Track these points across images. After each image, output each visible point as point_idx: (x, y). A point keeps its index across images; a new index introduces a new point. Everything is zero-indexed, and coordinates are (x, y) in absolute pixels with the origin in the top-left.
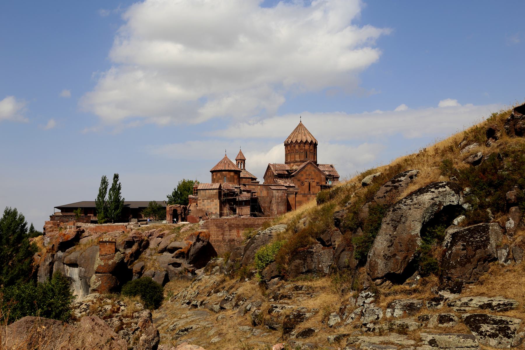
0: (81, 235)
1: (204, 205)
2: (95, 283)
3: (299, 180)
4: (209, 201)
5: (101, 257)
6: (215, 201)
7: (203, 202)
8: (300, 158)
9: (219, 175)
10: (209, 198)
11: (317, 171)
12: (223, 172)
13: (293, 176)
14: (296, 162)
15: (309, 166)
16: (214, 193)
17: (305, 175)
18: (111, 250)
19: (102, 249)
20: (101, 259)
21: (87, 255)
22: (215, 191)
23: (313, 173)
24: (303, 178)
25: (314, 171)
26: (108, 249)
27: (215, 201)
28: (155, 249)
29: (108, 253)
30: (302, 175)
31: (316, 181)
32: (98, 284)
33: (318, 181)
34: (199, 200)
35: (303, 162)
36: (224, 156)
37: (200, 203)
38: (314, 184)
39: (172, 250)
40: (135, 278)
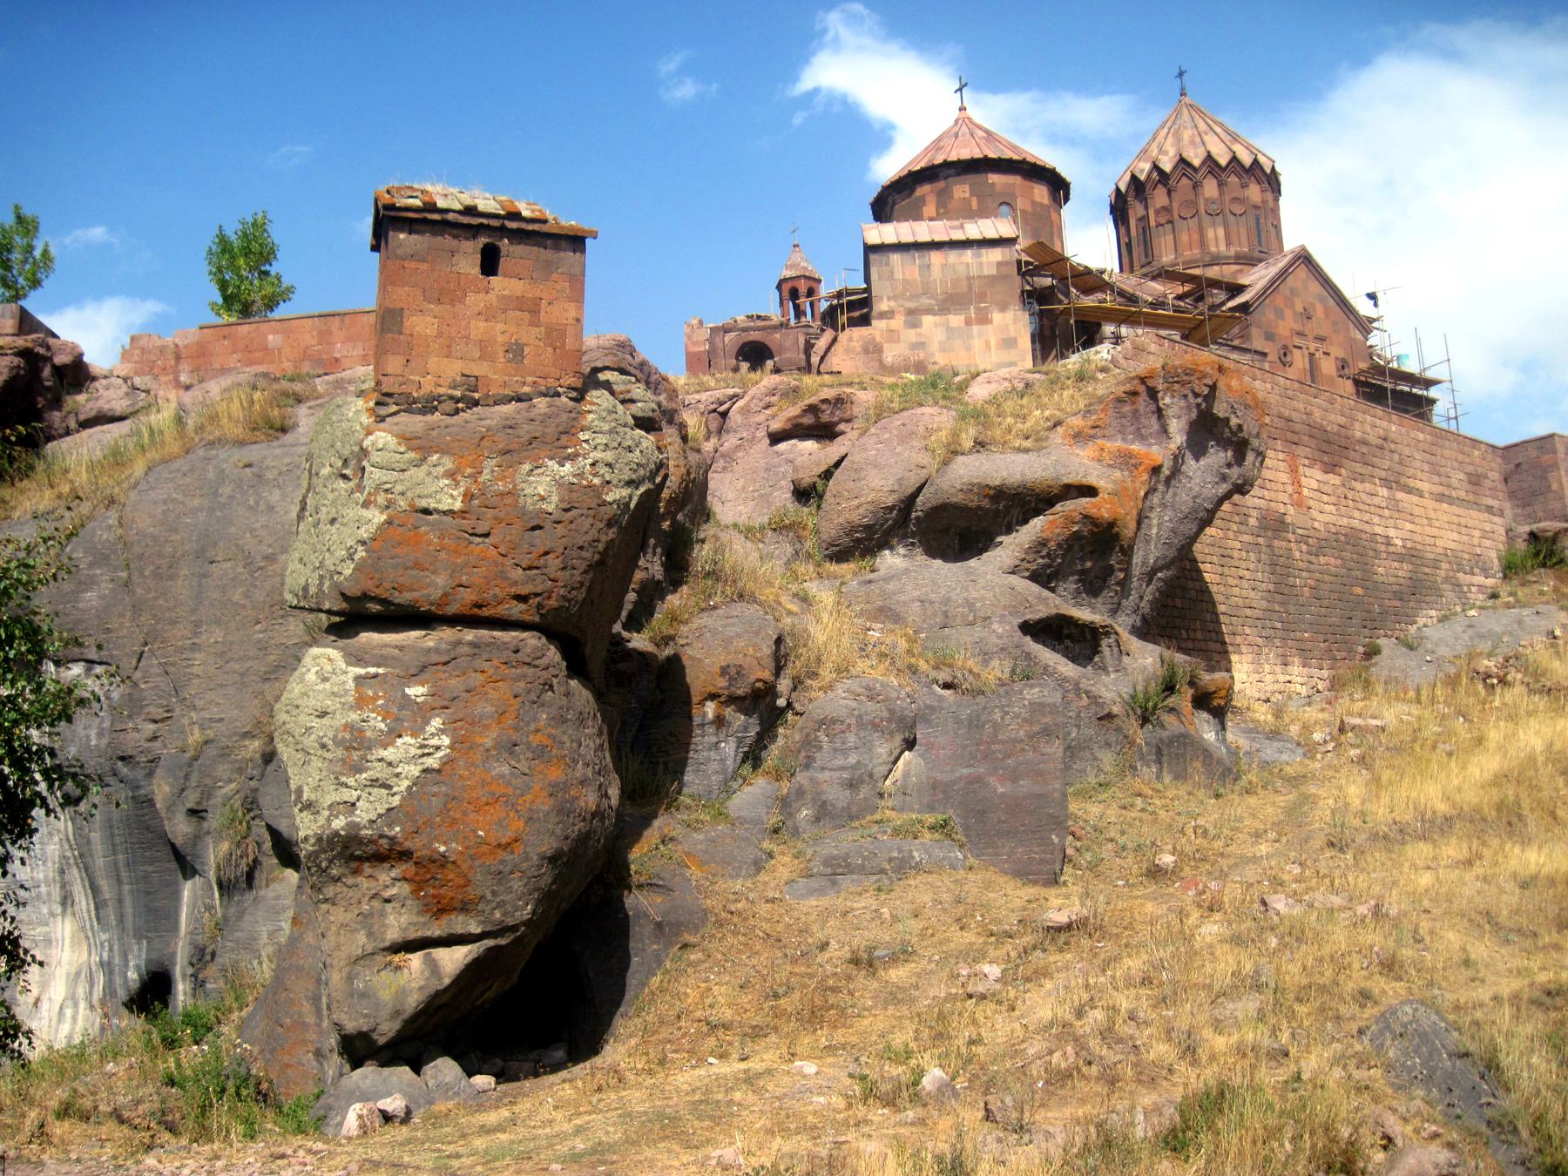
0: (57, 403)
1: (921, 345)
2: (356, 745)
3: (1270, 337)
4: (956, 320)
5: (415, 423)
6: (997, 317)
7: (916, 325)
8: (1228, 244)
9: (961, 190)
10: (950, 302)
11: (1331, 303)
12: (994, 178)
13: (1244, 308)
14: (1216, 260)
15: (1302, 272)
16: (990, 271)
17: (1288, 313)
18: (531, 336)
19: (422, 324)
20: (421, 447)
21: (144, 522)
22: (995, 255)
23: (1319, 308)
24: (1286, 326)
25: (1322, 301)
26: (501, 332)
27: (997, 317)
28: (781, 527)
29: (495, 375)
30: (1280, 314)
31: (1337, 352)
32: (406, 757)
33: (1341, 355)
34: (883, 315)
35: (1250, 261)
36: (956, 114)
37: (893, 336)
38: (1328, 367)
39: (957, 529)
40: (714, 750)
